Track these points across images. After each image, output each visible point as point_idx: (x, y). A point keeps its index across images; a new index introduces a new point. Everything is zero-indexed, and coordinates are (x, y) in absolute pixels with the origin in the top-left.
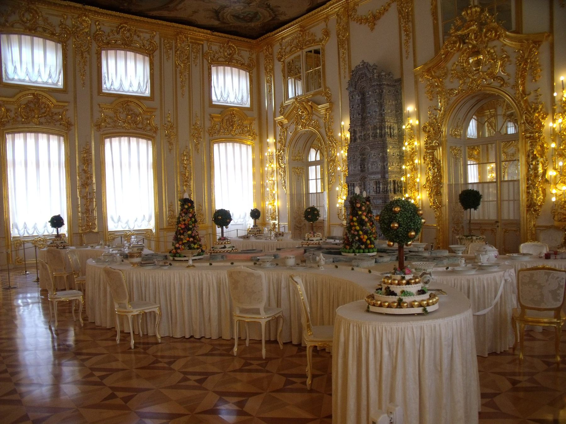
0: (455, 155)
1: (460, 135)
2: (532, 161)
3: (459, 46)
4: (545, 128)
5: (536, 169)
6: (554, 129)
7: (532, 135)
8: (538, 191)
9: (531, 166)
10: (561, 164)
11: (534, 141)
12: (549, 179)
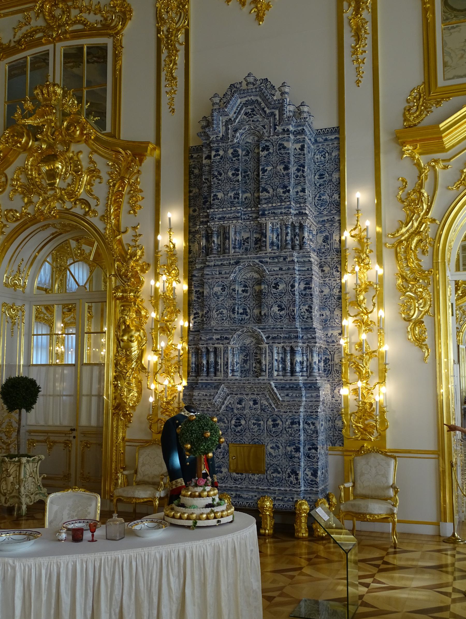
0: (11, 318)
1: (24, 287)
2: (123, 336)
3: (27, 143)
4: (145, 285)
5: (128, 348)
6: (156, 289)
7: (125, 295)
8: (129, 384)
9: (122, 343)
10: (163, 344)
11: (126, 303)
12: (146, 366)
